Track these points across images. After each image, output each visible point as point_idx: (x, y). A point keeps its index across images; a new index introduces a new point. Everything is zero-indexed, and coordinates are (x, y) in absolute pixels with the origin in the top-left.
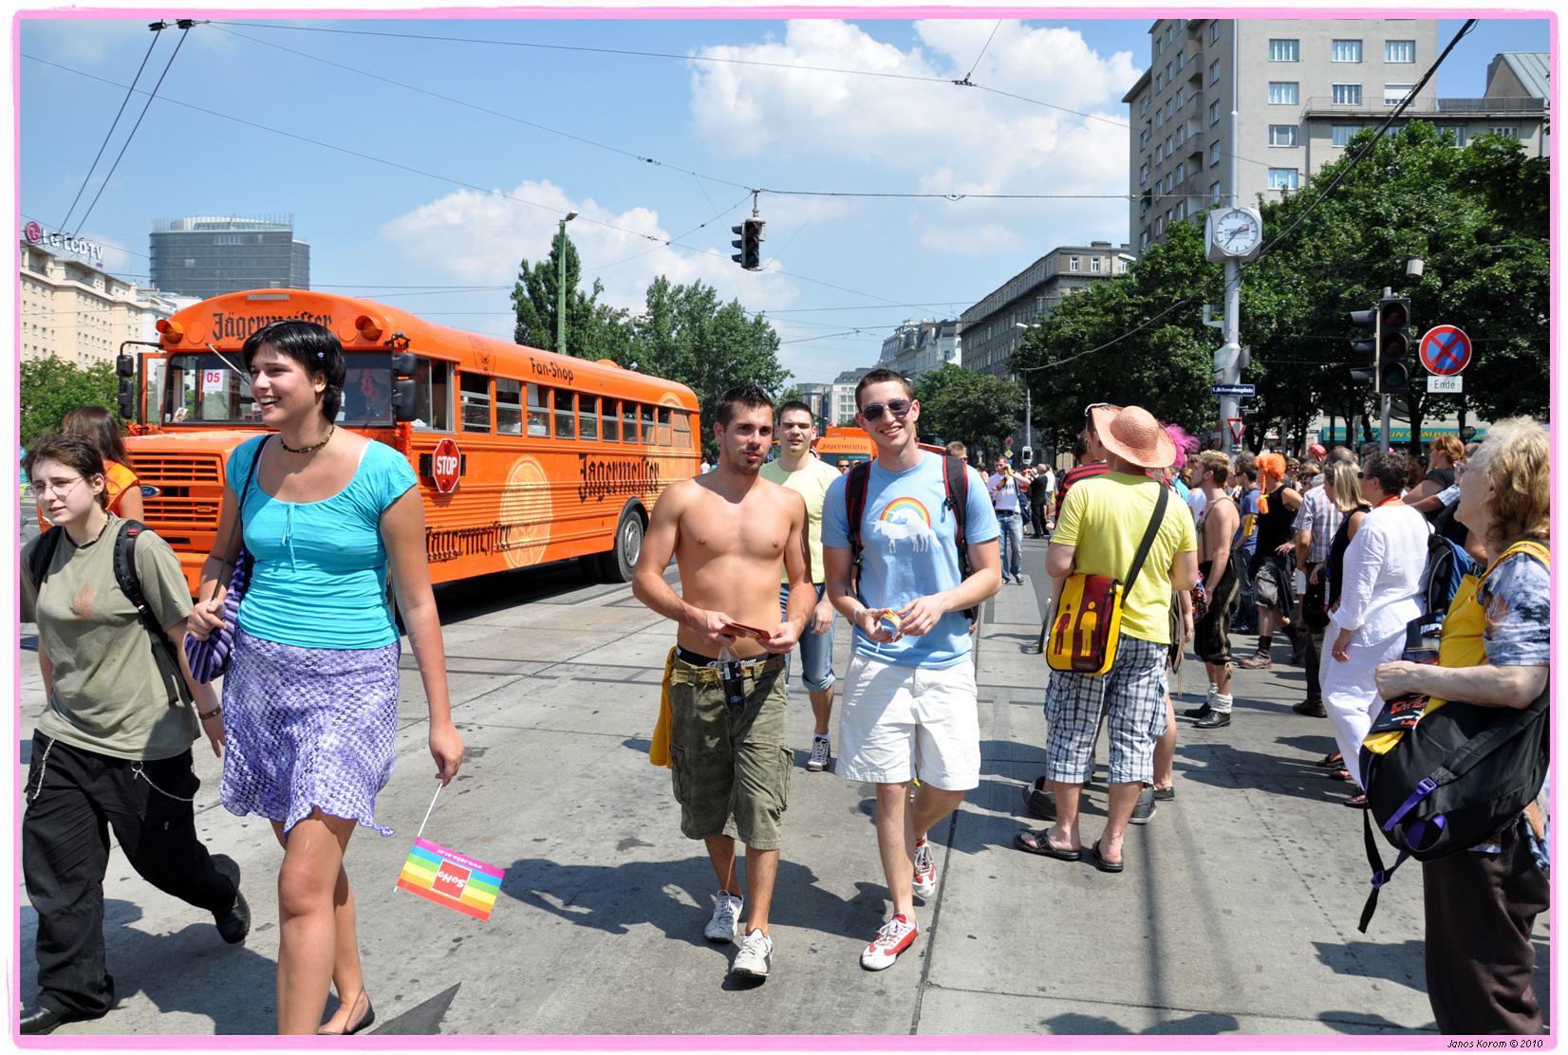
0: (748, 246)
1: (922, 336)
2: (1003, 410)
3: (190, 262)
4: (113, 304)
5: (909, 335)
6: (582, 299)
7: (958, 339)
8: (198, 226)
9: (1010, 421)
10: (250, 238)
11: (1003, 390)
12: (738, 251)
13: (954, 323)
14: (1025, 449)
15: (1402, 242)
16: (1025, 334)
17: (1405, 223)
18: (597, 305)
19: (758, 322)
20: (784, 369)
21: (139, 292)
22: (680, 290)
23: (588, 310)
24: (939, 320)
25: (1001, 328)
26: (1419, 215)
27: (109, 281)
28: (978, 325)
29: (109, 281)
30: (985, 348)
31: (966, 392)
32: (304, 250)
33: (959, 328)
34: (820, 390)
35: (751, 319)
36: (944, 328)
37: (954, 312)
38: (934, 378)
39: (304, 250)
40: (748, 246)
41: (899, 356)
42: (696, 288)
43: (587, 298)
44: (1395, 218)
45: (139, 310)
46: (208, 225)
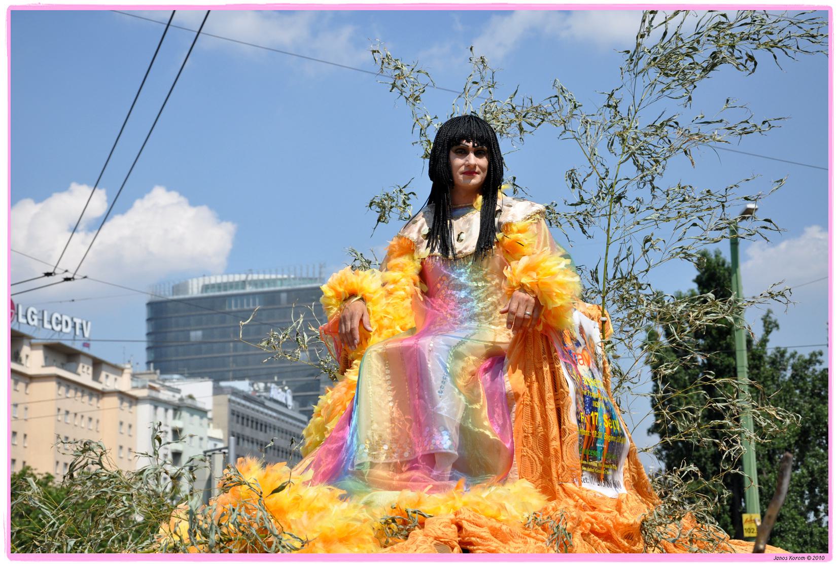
3: (196, 335)
4: (101, 394)
6: (749, 342)
18: (770, 350)
21: (134, 376)
23: (760, 358)
27: (97, 364)
29: (97, 364)
43: (756, 340)
45: (134, 400)
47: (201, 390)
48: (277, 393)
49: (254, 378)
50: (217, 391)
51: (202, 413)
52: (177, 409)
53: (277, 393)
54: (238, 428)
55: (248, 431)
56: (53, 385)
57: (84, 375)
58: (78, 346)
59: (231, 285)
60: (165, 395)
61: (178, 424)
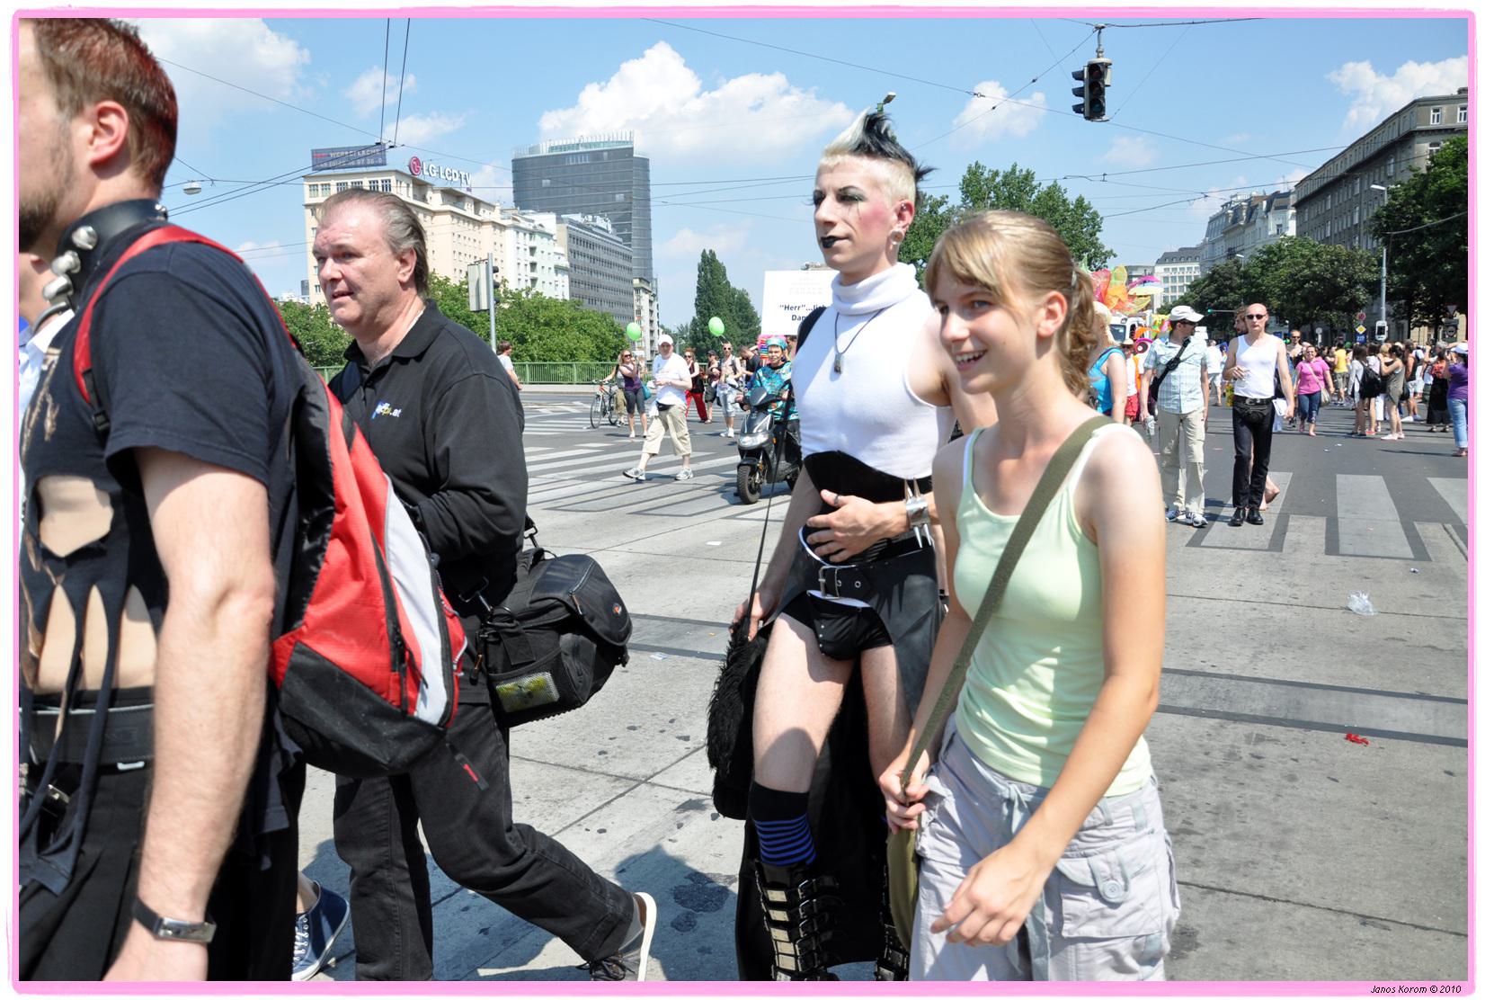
0: (1092, 93)
1: (1252, 208)
2: (1352, 283)
3: (546, 182)
4: (481, 223)
5: (1237, 210)
8: (552, 149)
9: (1362, 295)
10: (596, 156)
11: (1351, 259)
12: (1080, 100)
13: (1287, 195)
14: (1379, 324)
19: (1080, 201)
20: (1107, 248)
22: (996, 174)
24: (1269, 192)
25: (1343, 195)
27: (477, 203)
28: (1317, 195)
30: (1324, 220)
31: (1309, 266)
32: (644, 163)
33: (1293, 199)
34: (1141, 272)
35: (1071, 197)
36: (1276, 201)
37: (1290, 177)
38: (1269, 251)
39: (644, 163)
40: (1092, 93)
41: (1226, 233)
42: (1013, 171)
45: (503, 227)
46: (560, 148)
47: (548, 220)
48: (600, 222)
49: (585, 214)
50: (559, 220)
51: (550, 236)
52: (532, 233)
53: (600, 222)
54: (574, 247)
55: (581, 249)
56: (448, 217)
57: (469, 210)
58: (464, 191)
59: (570, 147)
60: (524, 224)
61: (533, 244)
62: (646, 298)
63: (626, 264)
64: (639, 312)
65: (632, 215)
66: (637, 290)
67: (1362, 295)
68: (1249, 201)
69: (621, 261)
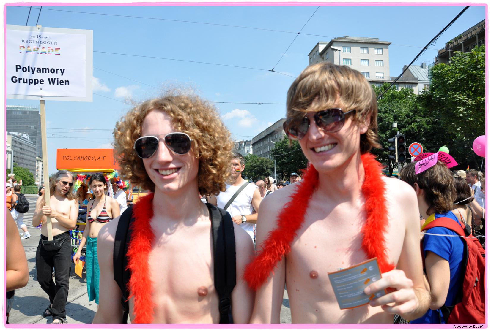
2: (267, 168)
5: (236, 145)
7: (251, 146)
9: (269, 171)
11: (267, 162)
13: (250, 141)
15: (386, 117)
16: (276, 144)
17: (386, 112)
24: (245, 140)
25: (265, 143)
26: (390, 110)
28: (258, 142)
30: (260, 149)
31: (256, 163)
33: (251, 143)
36: (247, 143)
44: (383, 110)
62: (41, 163)
63: (34, 151)
64: (38, 168)
65: (36, 135)
66: (38, 160)
67: (269, 171)
68: (239, 143)
69: (32, 150)
